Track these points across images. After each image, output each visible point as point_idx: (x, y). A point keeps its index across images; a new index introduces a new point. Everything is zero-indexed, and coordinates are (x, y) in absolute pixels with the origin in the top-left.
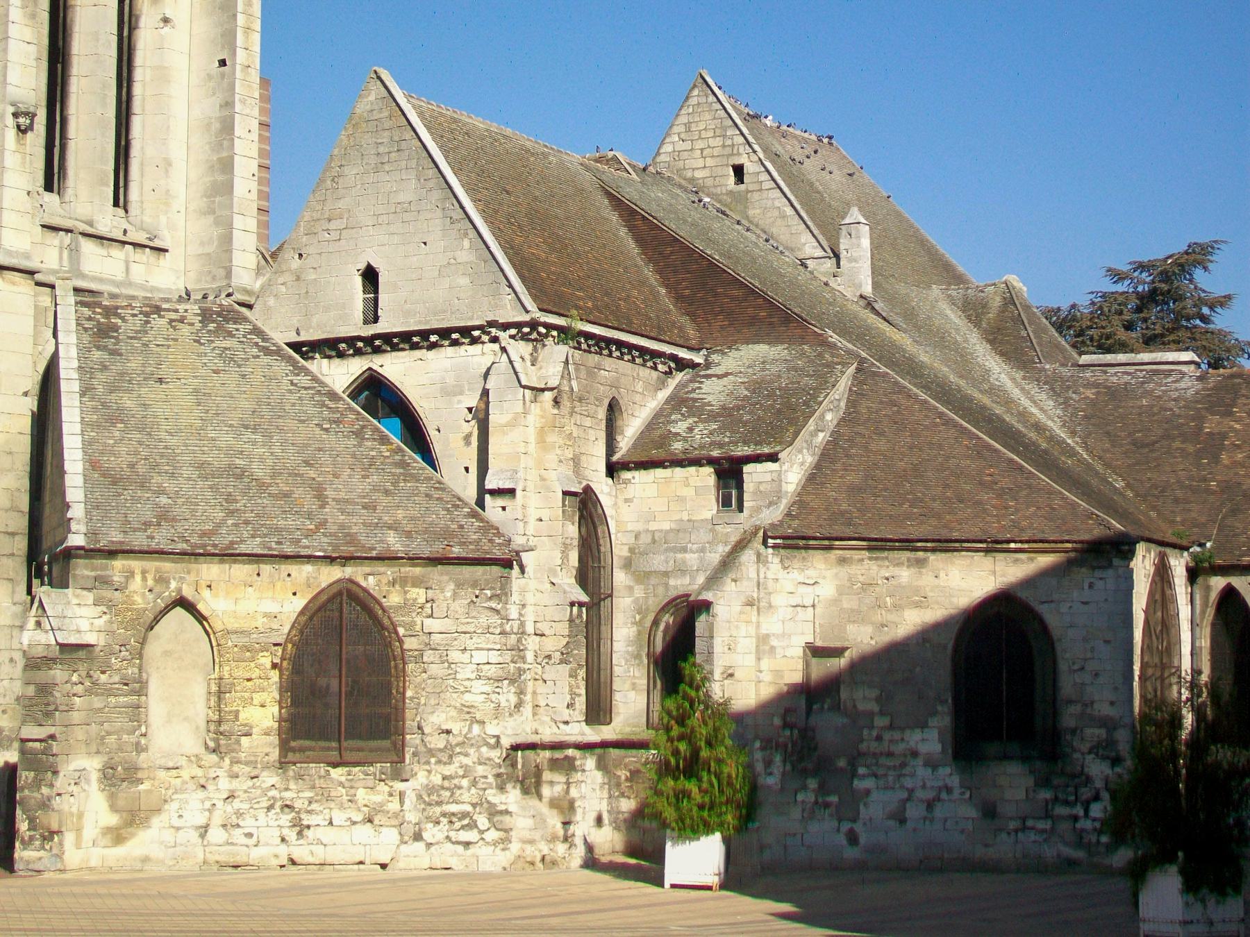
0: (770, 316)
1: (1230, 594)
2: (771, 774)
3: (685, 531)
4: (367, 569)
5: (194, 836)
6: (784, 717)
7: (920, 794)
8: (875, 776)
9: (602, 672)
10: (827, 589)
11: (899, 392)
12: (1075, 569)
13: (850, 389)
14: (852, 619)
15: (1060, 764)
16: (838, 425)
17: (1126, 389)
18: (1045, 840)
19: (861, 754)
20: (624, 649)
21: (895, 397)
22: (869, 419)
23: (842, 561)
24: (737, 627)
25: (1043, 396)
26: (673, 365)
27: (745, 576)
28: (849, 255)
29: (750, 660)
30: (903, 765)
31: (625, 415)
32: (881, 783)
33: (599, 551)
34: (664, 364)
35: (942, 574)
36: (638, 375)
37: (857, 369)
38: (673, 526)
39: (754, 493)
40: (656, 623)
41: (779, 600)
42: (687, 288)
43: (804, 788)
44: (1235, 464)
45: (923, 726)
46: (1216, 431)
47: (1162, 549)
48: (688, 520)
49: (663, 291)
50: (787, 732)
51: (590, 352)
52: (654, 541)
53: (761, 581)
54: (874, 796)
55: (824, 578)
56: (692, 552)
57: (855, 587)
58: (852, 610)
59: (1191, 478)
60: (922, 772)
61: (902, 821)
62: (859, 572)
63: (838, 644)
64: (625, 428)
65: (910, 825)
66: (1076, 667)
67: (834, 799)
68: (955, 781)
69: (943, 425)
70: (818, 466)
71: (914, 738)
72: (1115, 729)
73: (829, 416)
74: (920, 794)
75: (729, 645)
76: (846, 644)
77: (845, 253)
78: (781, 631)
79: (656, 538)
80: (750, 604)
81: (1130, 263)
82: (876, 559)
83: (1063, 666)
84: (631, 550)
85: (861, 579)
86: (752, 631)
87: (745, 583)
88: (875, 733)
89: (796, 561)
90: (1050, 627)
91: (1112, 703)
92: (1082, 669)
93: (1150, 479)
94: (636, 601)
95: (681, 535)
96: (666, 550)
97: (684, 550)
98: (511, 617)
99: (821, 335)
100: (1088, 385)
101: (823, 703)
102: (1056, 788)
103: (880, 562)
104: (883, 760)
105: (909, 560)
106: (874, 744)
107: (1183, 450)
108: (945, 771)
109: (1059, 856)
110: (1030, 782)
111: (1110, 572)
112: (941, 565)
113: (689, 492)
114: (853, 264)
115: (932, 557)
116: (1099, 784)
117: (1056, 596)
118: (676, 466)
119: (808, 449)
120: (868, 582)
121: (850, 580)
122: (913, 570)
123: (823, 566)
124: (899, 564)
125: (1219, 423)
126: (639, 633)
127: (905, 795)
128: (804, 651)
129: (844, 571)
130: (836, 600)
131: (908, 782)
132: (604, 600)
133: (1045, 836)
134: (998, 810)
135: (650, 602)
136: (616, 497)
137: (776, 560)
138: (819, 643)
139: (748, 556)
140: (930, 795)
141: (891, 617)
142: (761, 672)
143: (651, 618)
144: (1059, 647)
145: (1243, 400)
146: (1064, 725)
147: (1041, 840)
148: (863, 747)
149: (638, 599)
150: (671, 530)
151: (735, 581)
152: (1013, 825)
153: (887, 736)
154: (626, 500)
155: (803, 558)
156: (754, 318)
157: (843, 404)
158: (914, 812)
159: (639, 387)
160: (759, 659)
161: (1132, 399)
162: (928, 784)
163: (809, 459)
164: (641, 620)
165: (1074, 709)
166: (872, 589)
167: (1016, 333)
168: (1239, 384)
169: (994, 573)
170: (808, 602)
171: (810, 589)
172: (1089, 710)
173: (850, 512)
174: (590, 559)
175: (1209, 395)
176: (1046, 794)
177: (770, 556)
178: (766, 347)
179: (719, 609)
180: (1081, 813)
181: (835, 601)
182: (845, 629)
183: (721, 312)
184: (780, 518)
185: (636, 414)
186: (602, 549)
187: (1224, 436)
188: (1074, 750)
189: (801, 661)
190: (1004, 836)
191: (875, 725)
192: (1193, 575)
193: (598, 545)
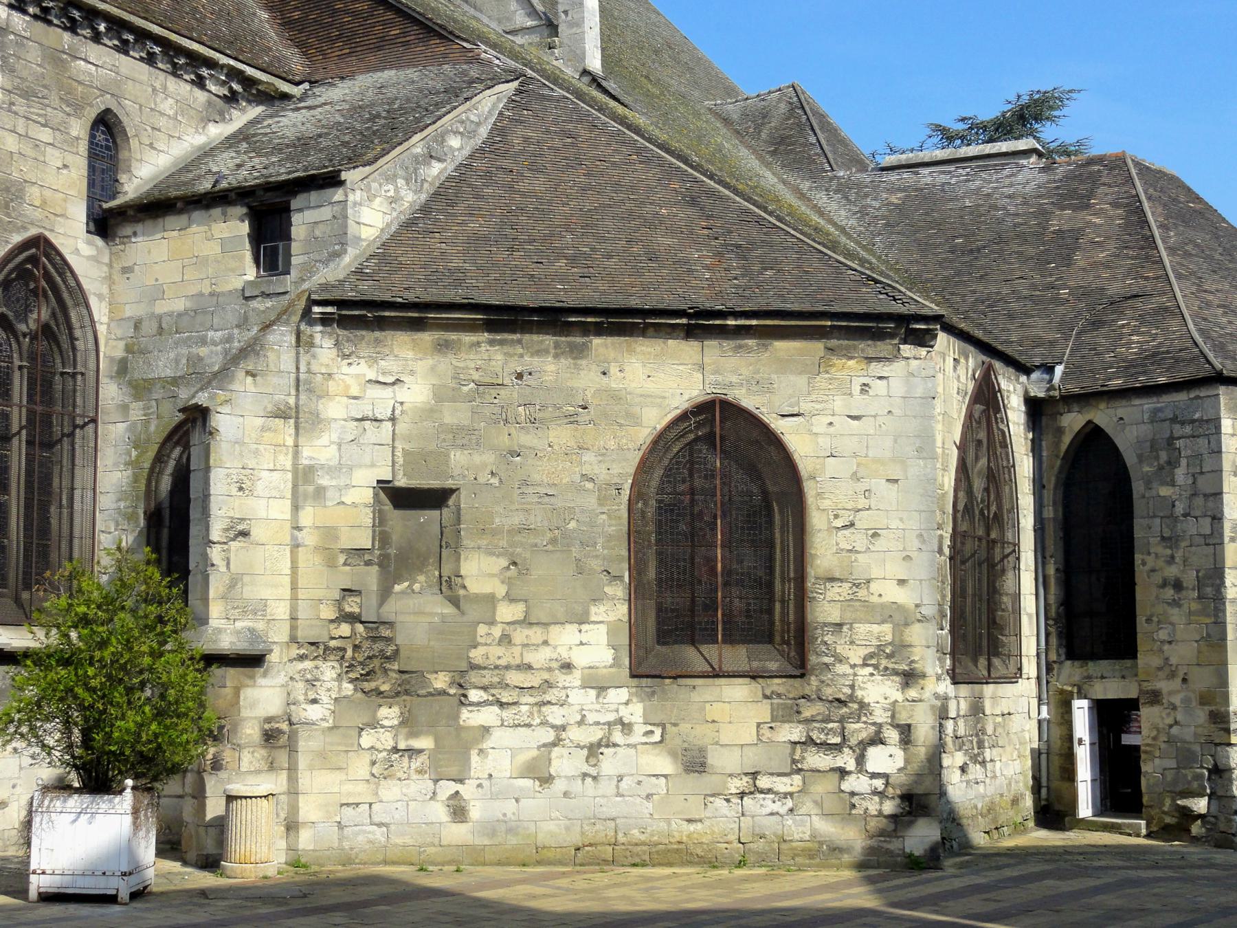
0: (404, 34)
1: (1093, 436)
2: (314, 701)
3: (204, 312)
6: (339, 603)
7: (576, 734)
8: (502, 705)
9: (76, 542)
10: (416, 393)
11: (580, 121)
12: (838, 362)
13: (501, 114)
14: (459, 442)
15: (814, 681)
16: (471, 156)
17: (943, 190)
18: (791, 810)
19: (474, 667)
20: (114, 506)
21: (570, 126)
22: (522, 152)
23: (443, 347)
24: (256, 453)
25: (834, 206)
26: (236, 87)
27: (272, 367)
28: (569, 18)
29: (281, 510)
30: (548, 684)
31: (134, 143)
32: (508, 714)
33: (74, 349)
34: (224, 83)
35: (614, 370)
36: (165, 88)
37: (516, 90)
38: (189, 305)
39: (307, 241)
40: (160, 459)
41: (335, 409)
42: (296, 9)
43: (374, 724)
44: (1095, 265)
45: (582, 619)
46: (1065, 227)
47: (987, 359)
48: (212, 294)
49: (265, 15)
50: (345, 629)
51: (49, 23)
52: (161, 331)
53: (302, 376)
54: (499, 737)
55: (412, 373)
56: (215, 344)
57: (465, 389)
58: (461, 428)
59: (1034, 287)
60: (582, 698)
61: (547, 780)
62: (473, 366)
63: (434, 484)
64: (134, 164)
65: (559, 786)
66: (839, 523)
67: (425, 743)
68: (635, 712)
69: (641, 162)
70: (425, 209)
71: (565, 639)
72: (907, 624)
73: (454, 142)
74: (576, 734)
75: (240, 482)
76: (449, 484)
77: (563, 16)
78: (334, 462)
79: (164, 325)
80: (281, 414)
81: (963, 120)
82: (502, 343)
83: (817, 520)
84: (128, 349)
85: (476, 376)
86: (287, 462)
87: (274, 380)
88: (497, 632)
89: (364, 344)
90: (796, 457)
91: (902, 582)
92: (852, 525)
93: (974, 292)
94: (131, 429)
95: (199, 318)
96: (177, 344)
97: (203, 342)
99: (471, 50)
100: (892, 190)
101: (414, 581)
102: (807, 721)
103: (506, 349)
104: (514, 678)
105: (557, 346)
106: (499, 651)
107: (1020, 253)
108: (617, 696)
109: (813, 836)
110: (763, 711)
111: (899, 366)
112: (612, 354)
113: (212, 249)
114: (574, 30)
115: (597, 341)
116: (880, 716)
117: (804, 407)
118: (196, 209)
119: (408, 181)
120: (488, 380)
121: (455, 377)
122: (565, 362)
123: (410, 355)
124: (538, 353)
125: (1070, 219)
126: (136, 480)
127: (550, 736)
128: (376, 495)
129: (446, 363)
130: (432, 410)
131: (555, 715)
132: (82, 427)
133: (789, 803)
134: (710, 761)
135: (152, 428)
136: (110, 266)
137: (328, 343)
138: (402, 482)
139: (282, 337)
140: (596, 735)
141: (527, 439)
142: (299, 529)
143: (151, 454)
144: (810, 489)
145: (1102, 189)
146: (821, 619)
147: (783, 810)
148: (476, 655)
149: (134, 424)
150: (186, 312)
151: (248, 373)
152: (735, 785)
153: (519, 635)
154: (126, 270)
155: (376, 339)
156: (382, 39)
157: (484, 131)
158: (566, 764)
159: (168, 106)
160: (296, 508)
161: (951, 200)
162: (591, 718)
163: (410, 198)
164: (138, 457)
165: (837, 591)
166: (494, 392)
167: (802, 140)
168: (1099, 171)
169: (702, 367)
170: (384, 412)
171: (387, 392)
172: (862, 593)
173: (458, 270)
174: (58, 361)
175: (1058, 188)
176: (794, 732)
177: (318, 337)
178: (393, 72)
179: (224, 422)
180: (851, 765)
181: (429, 412)
182: (448, 456)
183: (339, 37)
184: (341, 277)
185: (161, 146)
186: (80, 345)
187: (1077, 234)
188: (840, 659)
189: (369, 511)
190: (719, 802)
191: (498, 619)
192: (1036, 409)
193: (72, 339)
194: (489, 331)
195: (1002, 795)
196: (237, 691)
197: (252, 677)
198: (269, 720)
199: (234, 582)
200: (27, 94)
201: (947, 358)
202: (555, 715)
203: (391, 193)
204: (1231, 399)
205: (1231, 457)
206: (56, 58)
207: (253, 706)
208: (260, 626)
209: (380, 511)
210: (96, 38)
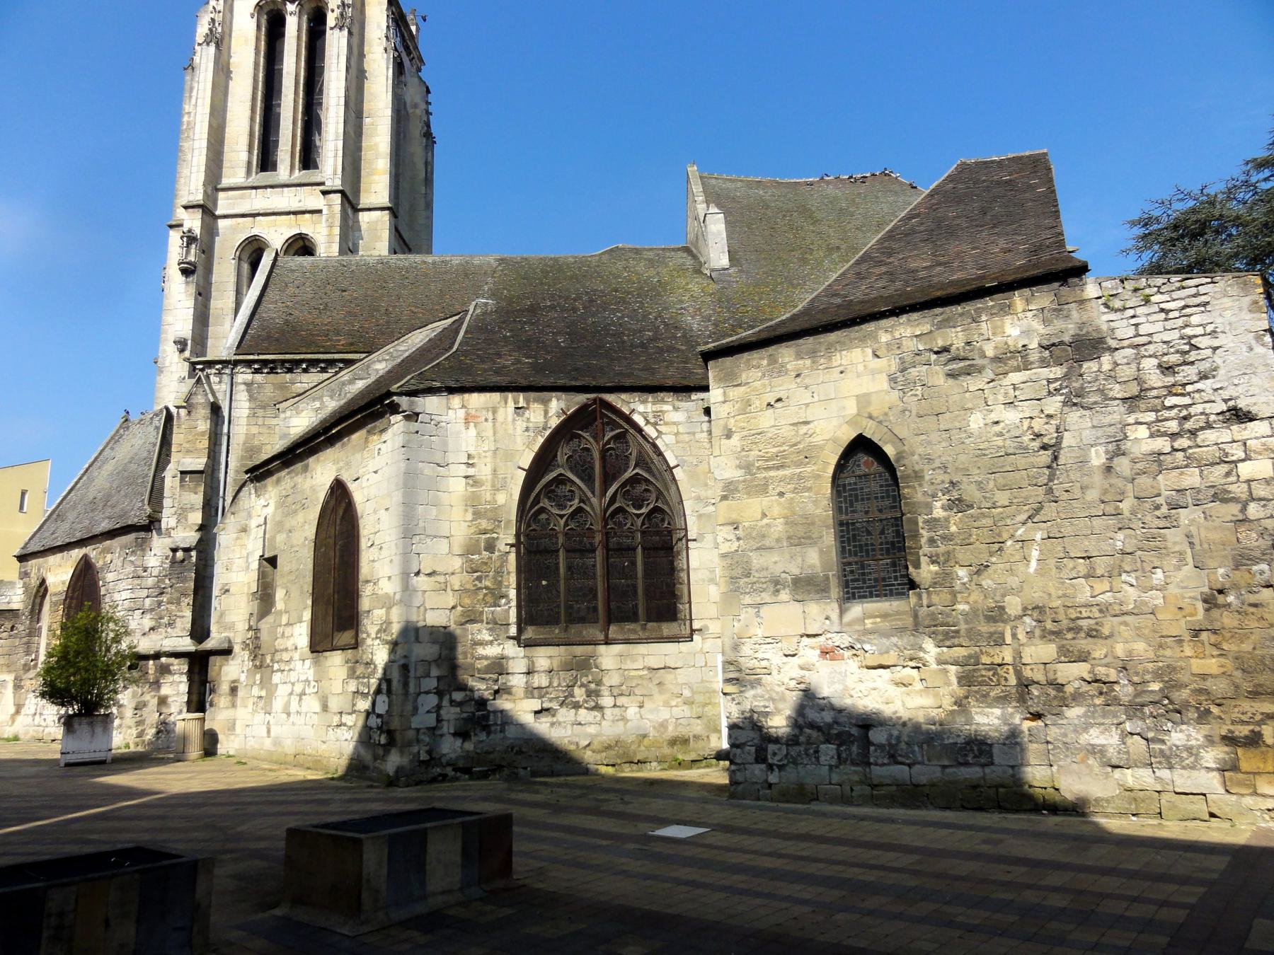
4: (93, 546)
5: (30, 718)
51: (277, 373)
98: (150, 565)
115: (311, 460)
194: (288, 467)
195: (645, 736)
196: (220, 667)
197: (227, 660)
198: (234, 682)
199: (222, 615)
200: (264, 407)
201: (501, 412)
202: (293, 677)
203: (318, 406)
204: (721, 370)
205: (722, 422)
206: (282, 387)
207: (227, 674)
208: (231, 635)
209: (263, 572)
210: (305, 371)
